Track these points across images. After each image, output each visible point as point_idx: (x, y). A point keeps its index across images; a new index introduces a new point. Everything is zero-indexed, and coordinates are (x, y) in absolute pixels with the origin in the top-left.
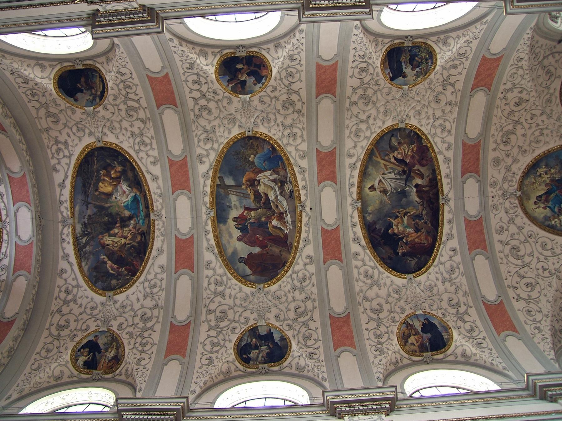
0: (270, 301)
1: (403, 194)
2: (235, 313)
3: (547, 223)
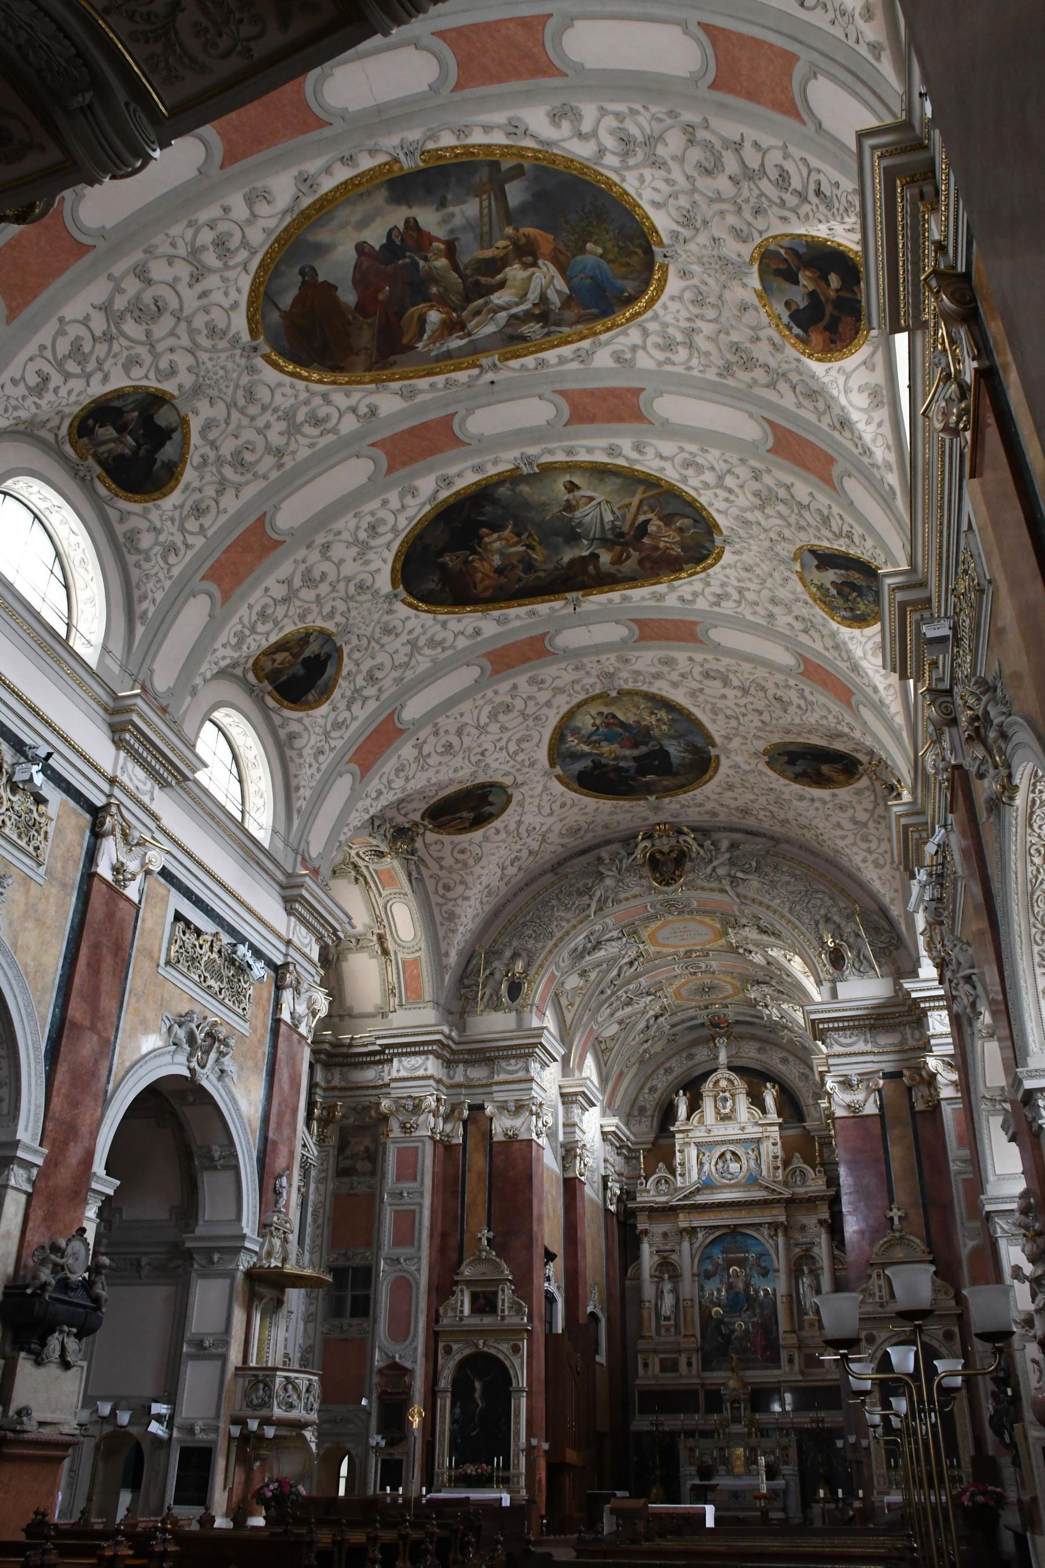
0: (237, 386)
1: (573, 536)
2: (172, 334)
3: (568, 733)
